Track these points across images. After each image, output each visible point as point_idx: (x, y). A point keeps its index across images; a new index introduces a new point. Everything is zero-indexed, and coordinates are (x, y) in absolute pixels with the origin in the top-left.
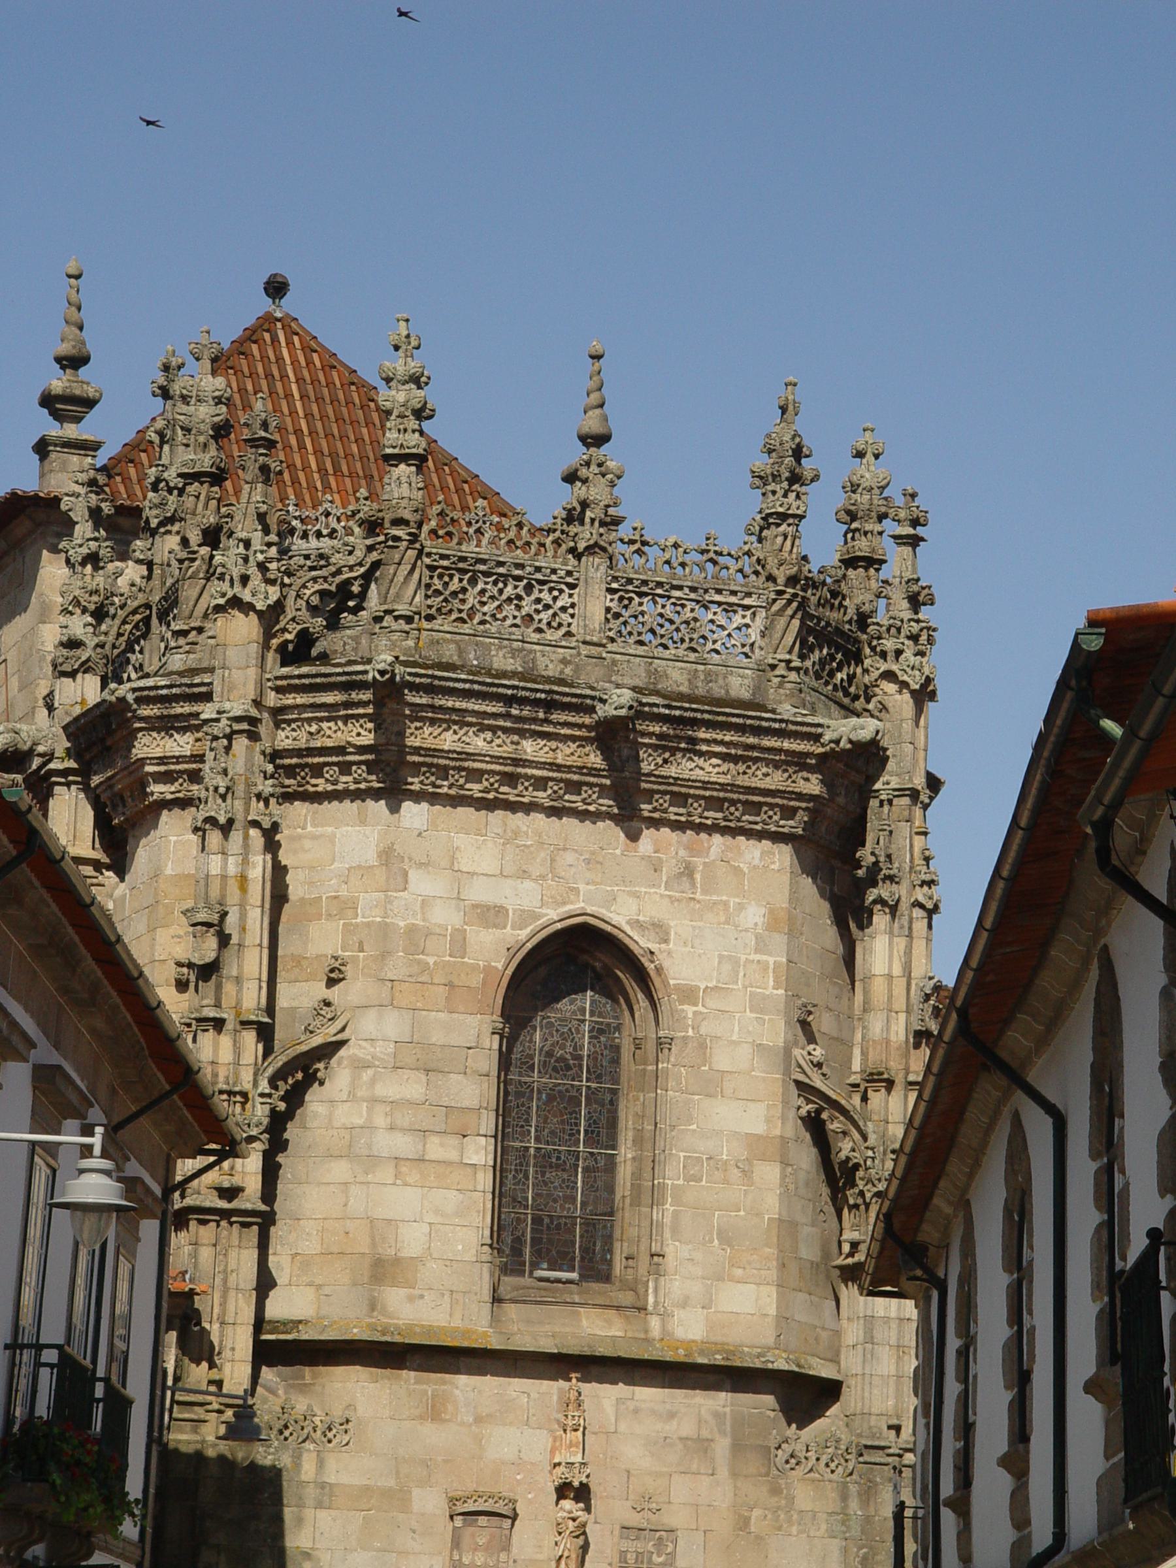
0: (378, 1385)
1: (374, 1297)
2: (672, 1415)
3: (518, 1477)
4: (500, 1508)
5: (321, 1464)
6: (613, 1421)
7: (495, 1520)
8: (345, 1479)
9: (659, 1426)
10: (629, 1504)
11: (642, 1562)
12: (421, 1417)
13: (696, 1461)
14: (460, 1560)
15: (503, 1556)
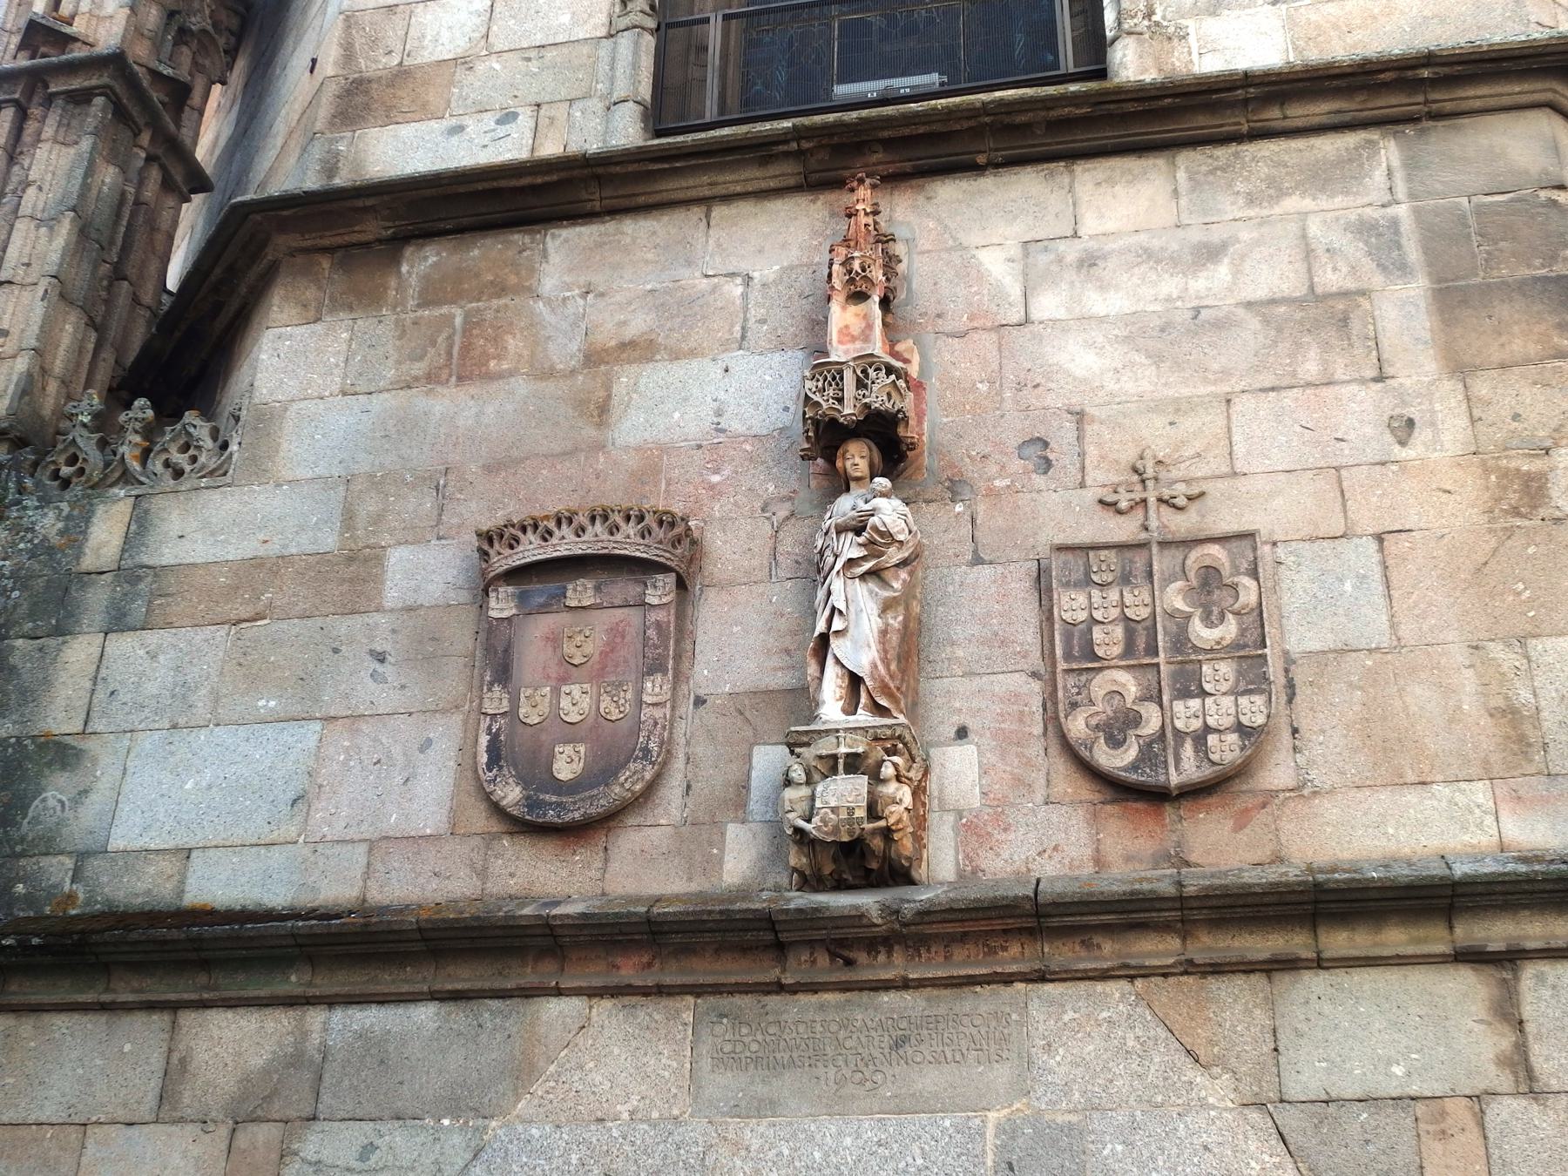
0: (318, 327)
1: (338, 153)
2: (1209, 254)
3: (716, 479)
4: (628, 542)
5: (139, 527)
6: (1015, 292)
7: (623, 588)
8: (198, 550)
9: (1170, 285)
10: (1091, 495)
11: (1153, 650)
12: (431, 378)
13: (1313, 353)
14: (512, 713)
15: (655, 688)
